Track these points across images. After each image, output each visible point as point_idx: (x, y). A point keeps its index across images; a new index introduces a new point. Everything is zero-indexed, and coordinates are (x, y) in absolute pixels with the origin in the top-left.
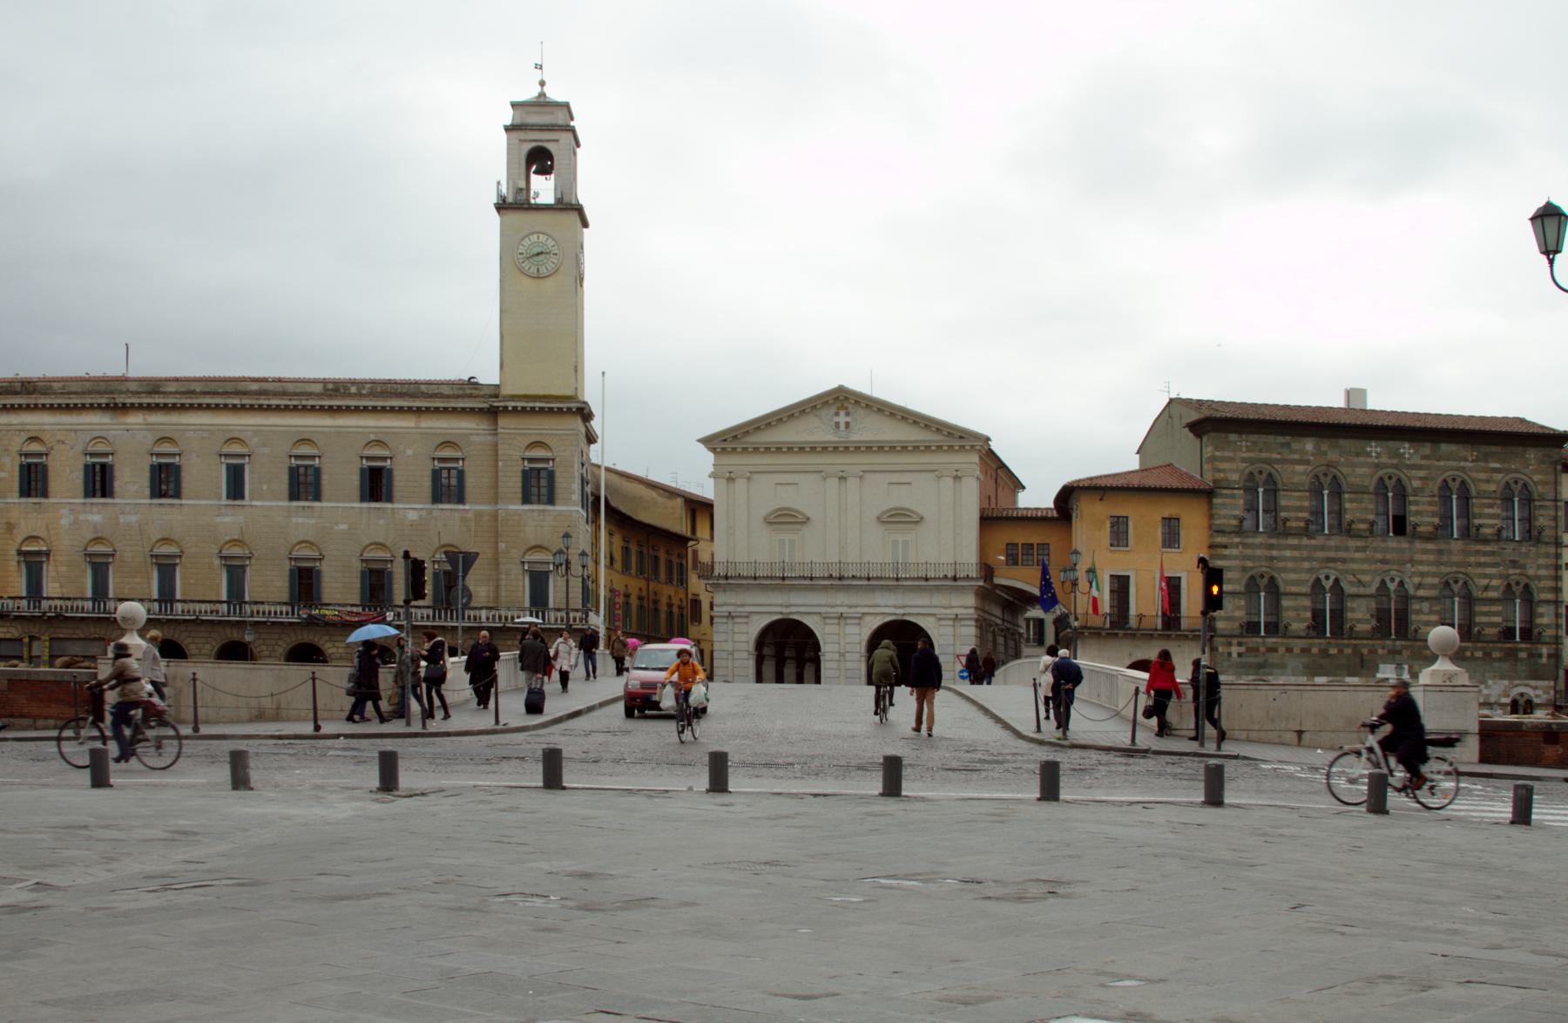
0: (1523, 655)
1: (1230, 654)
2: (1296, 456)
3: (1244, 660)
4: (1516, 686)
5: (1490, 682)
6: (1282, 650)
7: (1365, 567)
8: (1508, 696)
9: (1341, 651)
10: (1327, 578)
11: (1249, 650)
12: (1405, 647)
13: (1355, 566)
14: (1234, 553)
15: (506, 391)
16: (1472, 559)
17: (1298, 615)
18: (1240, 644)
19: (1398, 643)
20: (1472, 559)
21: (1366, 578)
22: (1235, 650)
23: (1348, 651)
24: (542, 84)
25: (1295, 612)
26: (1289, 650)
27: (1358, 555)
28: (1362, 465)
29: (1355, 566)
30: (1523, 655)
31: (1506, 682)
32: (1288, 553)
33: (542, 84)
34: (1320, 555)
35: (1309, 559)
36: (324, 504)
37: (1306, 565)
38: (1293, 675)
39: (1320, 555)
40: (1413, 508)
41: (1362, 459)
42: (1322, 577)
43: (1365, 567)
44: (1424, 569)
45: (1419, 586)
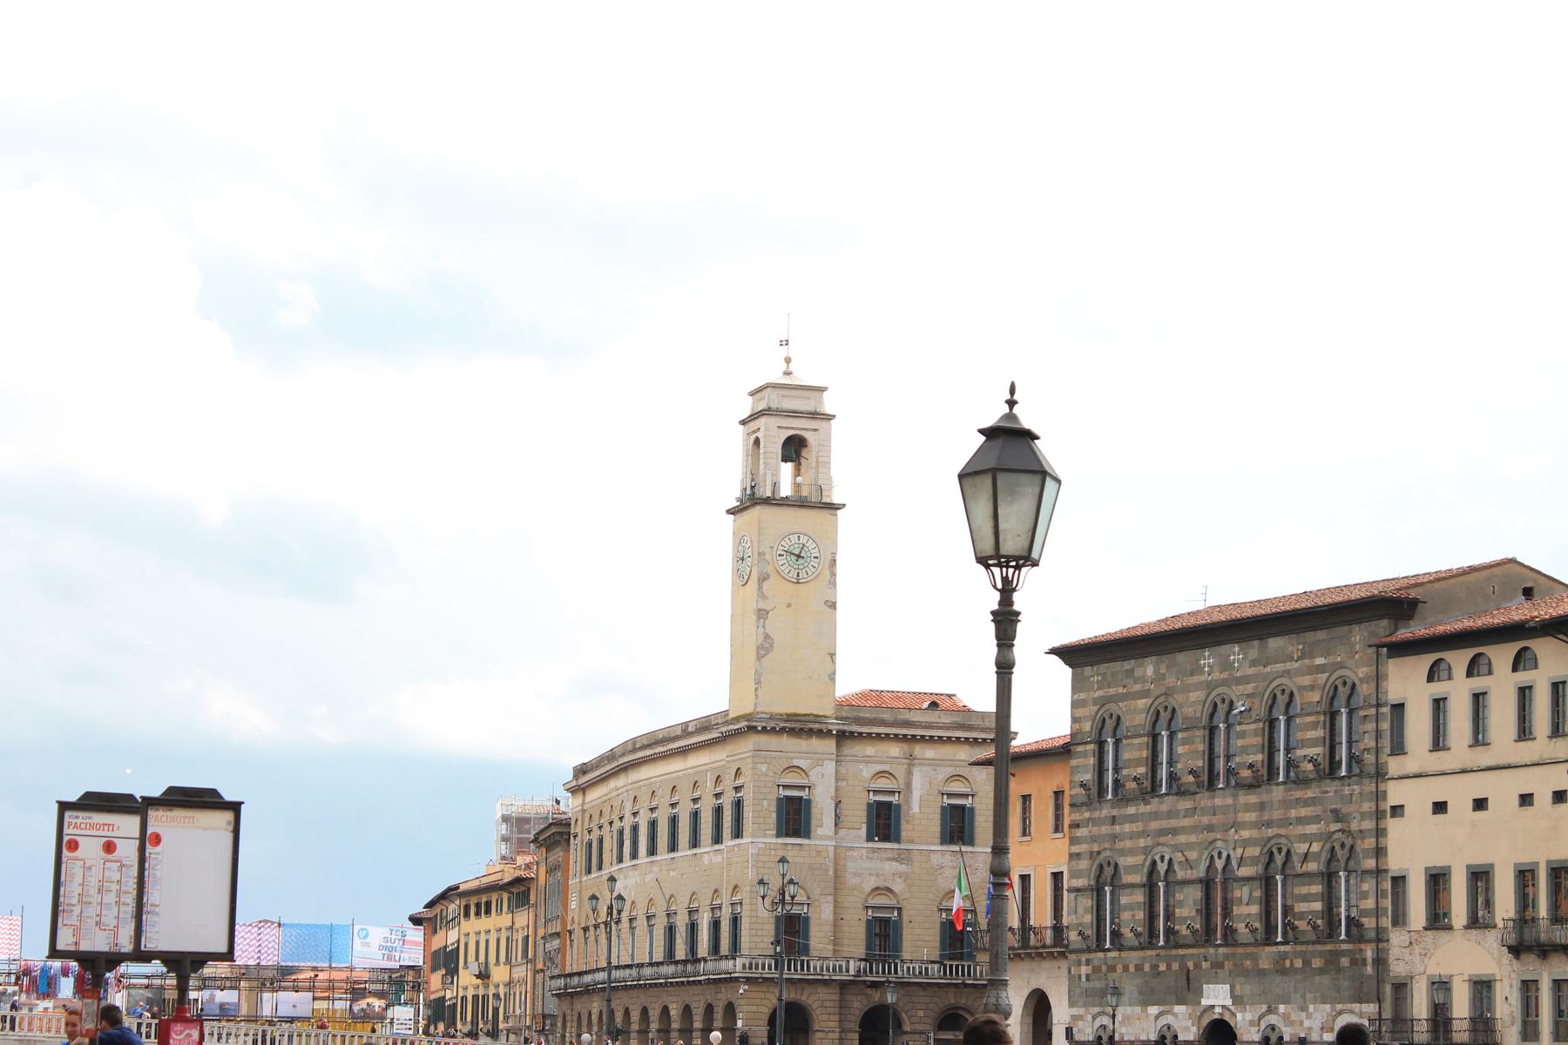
0: (1345, 961)
1: (1080, 976)
2: (1138, 687)
3: (1091, 985)
4: (1340, 1013)
5: (1311, 1008)
6: (1119, 968)
7: (1193, 839)
8: (1332, 1030)
9: (1169, 967)
10: (1162, 858)
11: (1096, 969)
12: (1227, 956)
13: (1182, 839)
14: (1084, 834)
15: (732, 715)
16: (1293, 813)
17: (1133, 916)
18: (1088, 962)
19: (1221, 950)
20: (1293, 813)
21: (1193, 855)
22: (1084, 970)
23: (1175, 966)
24: (788, 361)
25: (1131, 913)
26: (1126, 968)
27: (1186, 822)
28: (1197, 687)
29: (1182, 839)
30: (1345, 961)
31: (1328, 1007)
32: (1127, 828)
33: (788, 361)
34: (1154, 825)
35: (1143, 834)
36: (702, 850)
37: (1142, 842)
38: (1130, 1005)
39: (1154, 825)
40: (1240, 743)
41: (1195, 679)
42: (1157, 858)
43: (1193, 839)
44: (1246, 834)
45: (1241, 861)
